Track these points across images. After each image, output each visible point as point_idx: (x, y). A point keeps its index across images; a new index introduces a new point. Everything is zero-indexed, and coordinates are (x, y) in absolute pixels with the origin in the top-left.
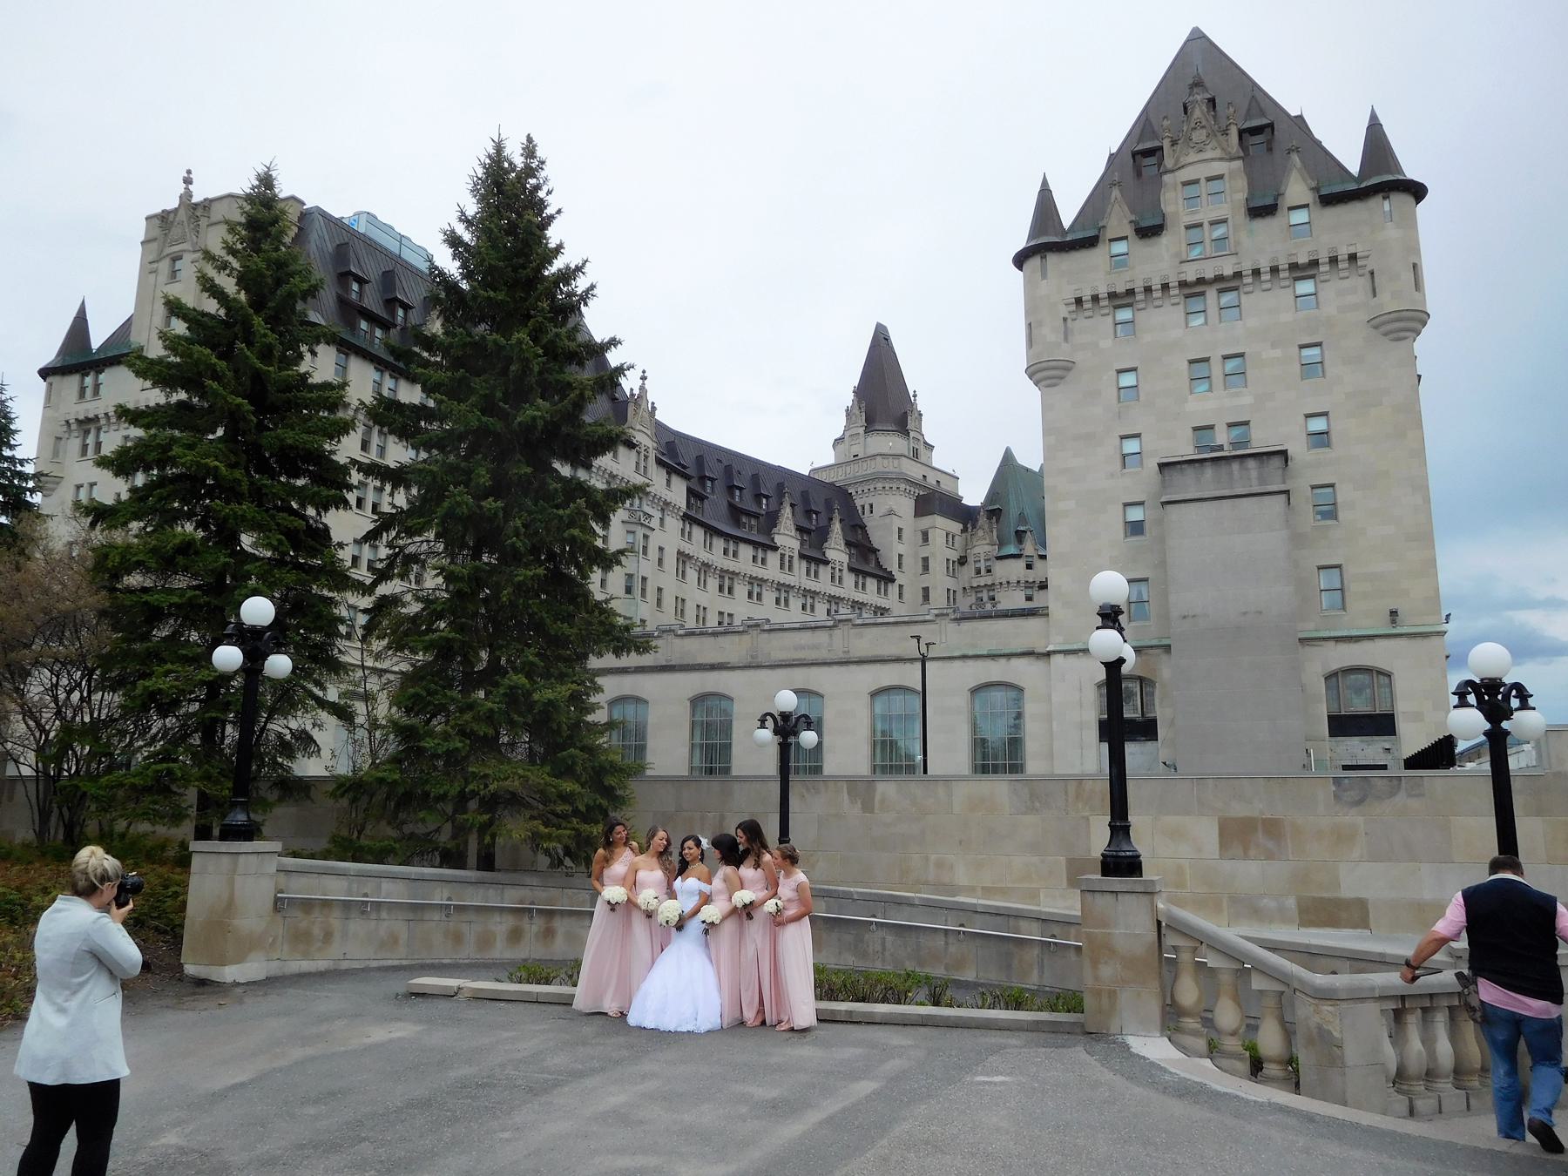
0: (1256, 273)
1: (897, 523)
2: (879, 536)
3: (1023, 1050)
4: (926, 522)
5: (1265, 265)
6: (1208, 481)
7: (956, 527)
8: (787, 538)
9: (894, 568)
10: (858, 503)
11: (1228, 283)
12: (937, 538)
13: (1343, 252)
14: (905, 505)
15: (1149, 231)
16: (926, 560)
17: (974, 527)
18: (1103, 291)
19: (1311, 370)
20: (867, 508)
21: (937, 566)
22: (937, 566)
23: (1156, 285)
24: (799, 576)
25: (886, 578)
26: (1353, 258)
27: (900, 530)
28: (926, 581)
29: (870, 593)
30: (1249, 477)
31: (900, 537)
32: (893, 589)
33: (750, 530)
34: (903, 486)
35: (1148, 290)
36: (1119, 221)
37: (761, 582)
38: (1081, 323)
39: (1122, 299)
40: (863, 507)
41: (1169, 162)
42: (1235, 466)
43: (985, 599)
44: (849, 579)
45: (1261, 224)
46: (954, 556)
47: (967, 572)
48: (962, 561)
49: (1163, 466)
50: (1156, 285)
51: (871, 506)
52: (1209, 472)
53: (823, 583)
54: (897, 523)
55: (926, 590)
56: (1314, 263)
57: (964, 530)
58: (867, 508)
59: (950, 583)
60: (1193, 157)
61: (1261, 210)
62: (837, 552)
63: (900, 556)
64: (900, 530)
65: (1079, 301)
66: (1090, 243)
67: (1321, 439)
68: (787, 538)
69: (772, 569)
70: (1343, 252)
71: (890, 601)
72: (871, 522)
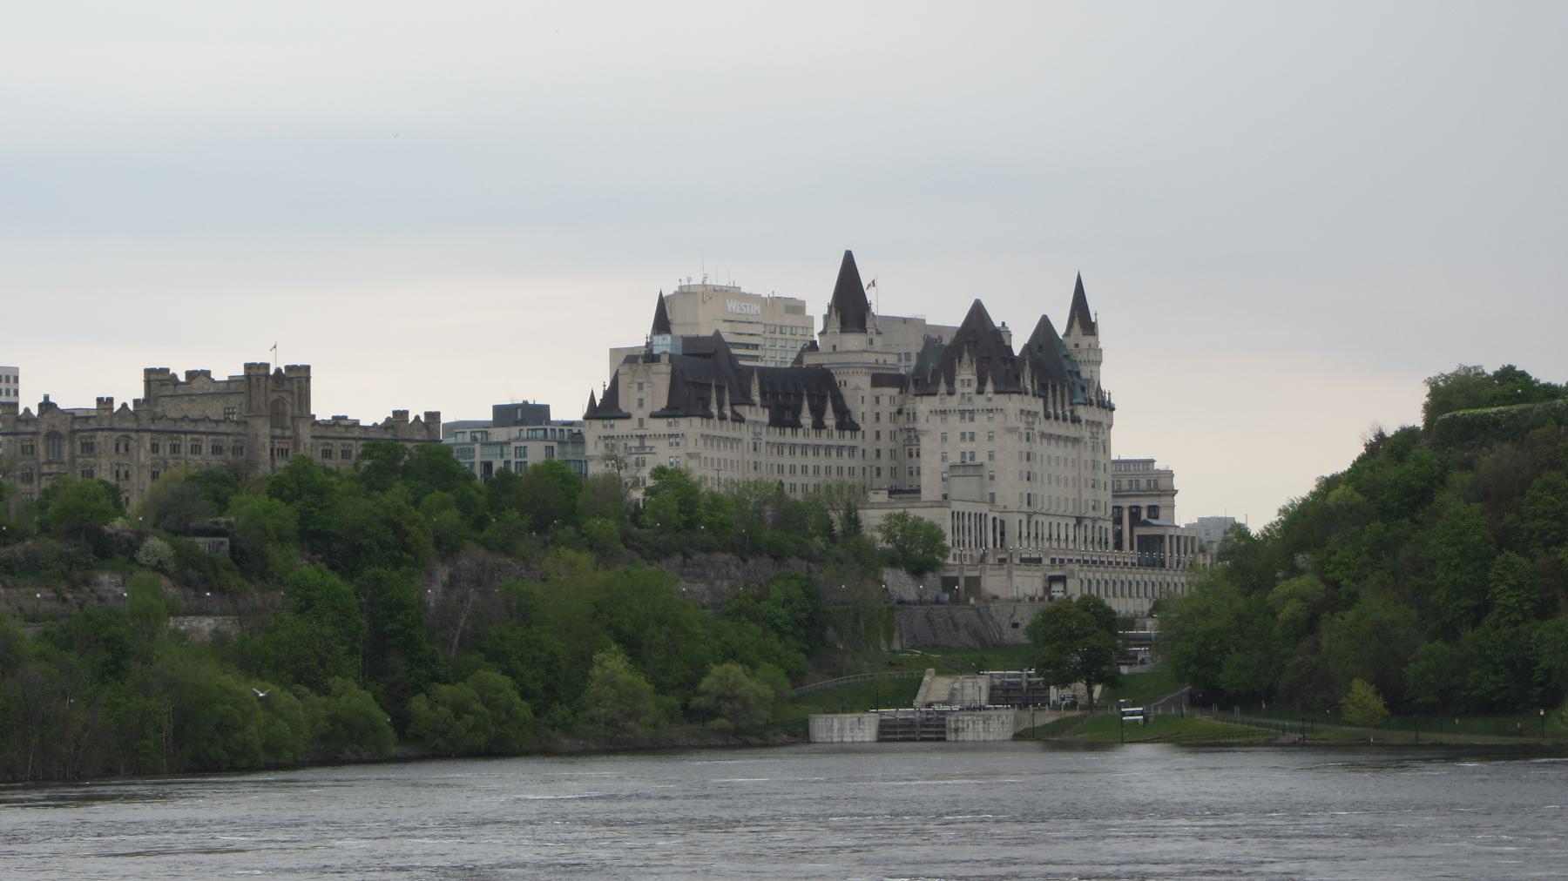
0: (978, 410)
1: (861, 393)
2: (851, 402)
3: (964, 839)
4: (878, 391)
5: (980, 408)
6: (960, 471)
7: (895, 391)
8: (806, 419)
9: (859, 421)
10: (838, 379)
11: (972, 412)
12: (885, 400)
13: (999, 408)
14: (864, 381)
15: (951, 393)
16: (878, 414)
17: (906, 391)
18: (938, 410)
19: (990, 438)
20: (843, 383)
21: (884, 418)
22: (884, 418)
23: (952, 410)
24: (812, 439)
25: (855, 428)
26: (1001, 409)
27: (863, 397)
28: (879, 427)
29: (847, 439)
30: (971, 471)
31: (863, 402)
32: (859, 434)
33: (788, 416)
34: (864, 371)
35: (950, 411)
36: (943, 388)
37: (795, 445)
38: (931, 418)
39: (944, 412)
40: (840, 382)
41: (957, 372)
42: (968, 468)
43: (913, 436)
44: (836, 433)
45: (979, 396)
46: (895, 409)
47: (902, 419)
48: (900, 412)
49: (951, 466)
50: (952, 410)
51: (845, 382)
52: (961, 468)
53: (824, 440)
54: (861, 393)
55: (878, 433)
56: (992, 410)
57: (901, 393)
58: (843, 383)
59: (892, 427)
60: (963, 372)
61: (980, 392)
62: (830, 420)
63: (863, 413)
64: (863, 397)
65: (931, 411)
66: (935, 394)
67: (991, 457)
68: (806, 419)
69: (800, 439)
70: (999, 408)
71: (858, 442)
72: (845, 391)
